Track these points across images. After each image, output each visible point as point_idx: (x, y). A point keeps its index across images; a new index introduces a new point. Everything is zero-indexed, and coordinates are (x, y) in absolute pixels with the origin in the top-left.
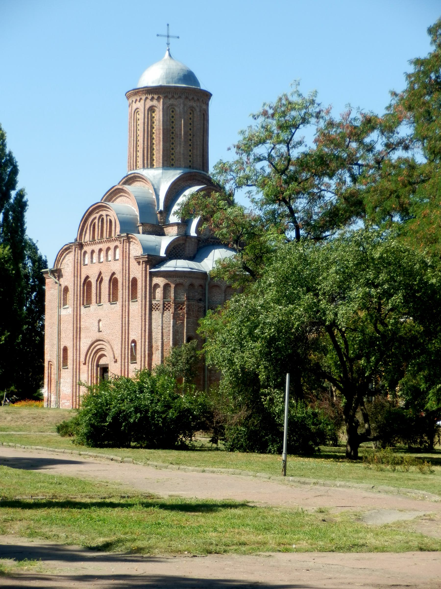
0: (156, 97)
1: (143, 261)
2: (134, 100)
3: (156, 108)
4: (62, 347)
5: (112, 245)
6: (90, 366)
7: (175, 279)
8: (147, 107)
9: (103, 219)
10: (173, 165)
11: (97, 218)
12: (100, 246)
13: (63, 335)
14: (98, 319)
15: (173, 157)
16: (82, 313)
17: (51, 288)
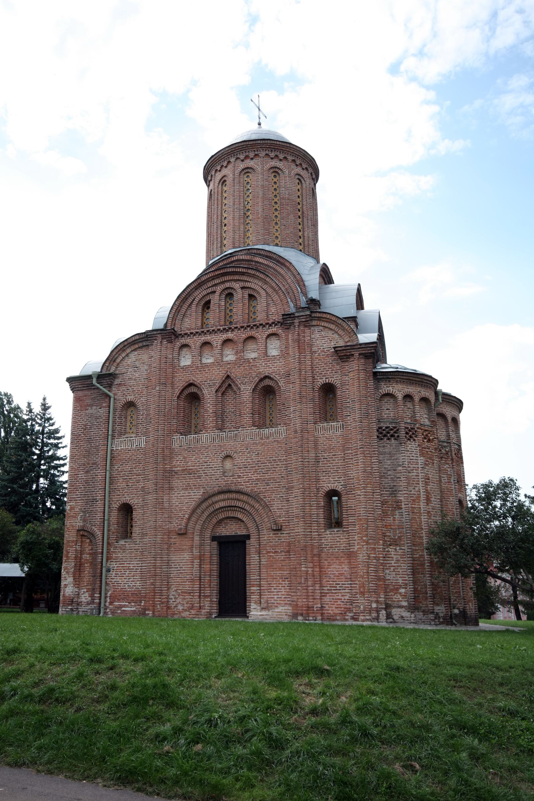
0: (281, 156)
1: (360, 354)
2: (242, 157)
3: (280, 172)
4: (116, 506)
5: (261, 334)
6: (197, 538)
7: (419, 389)
8: (268, 166)
9: (230, 295)
10: (301, 250)
11: (217, 294)
12: (230, 335)
13: (121, 484)
14: (223, 455)
15: (301, 241)
16: (176, 445)
17: (91, 406)
